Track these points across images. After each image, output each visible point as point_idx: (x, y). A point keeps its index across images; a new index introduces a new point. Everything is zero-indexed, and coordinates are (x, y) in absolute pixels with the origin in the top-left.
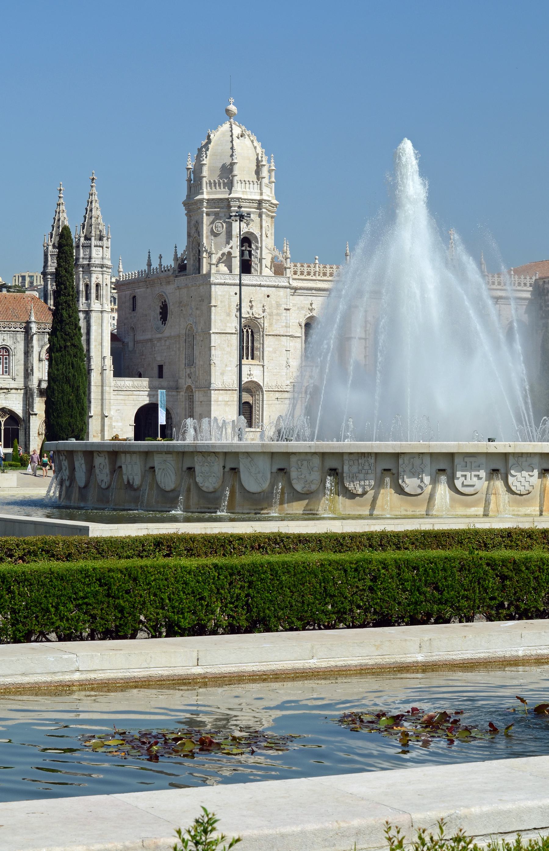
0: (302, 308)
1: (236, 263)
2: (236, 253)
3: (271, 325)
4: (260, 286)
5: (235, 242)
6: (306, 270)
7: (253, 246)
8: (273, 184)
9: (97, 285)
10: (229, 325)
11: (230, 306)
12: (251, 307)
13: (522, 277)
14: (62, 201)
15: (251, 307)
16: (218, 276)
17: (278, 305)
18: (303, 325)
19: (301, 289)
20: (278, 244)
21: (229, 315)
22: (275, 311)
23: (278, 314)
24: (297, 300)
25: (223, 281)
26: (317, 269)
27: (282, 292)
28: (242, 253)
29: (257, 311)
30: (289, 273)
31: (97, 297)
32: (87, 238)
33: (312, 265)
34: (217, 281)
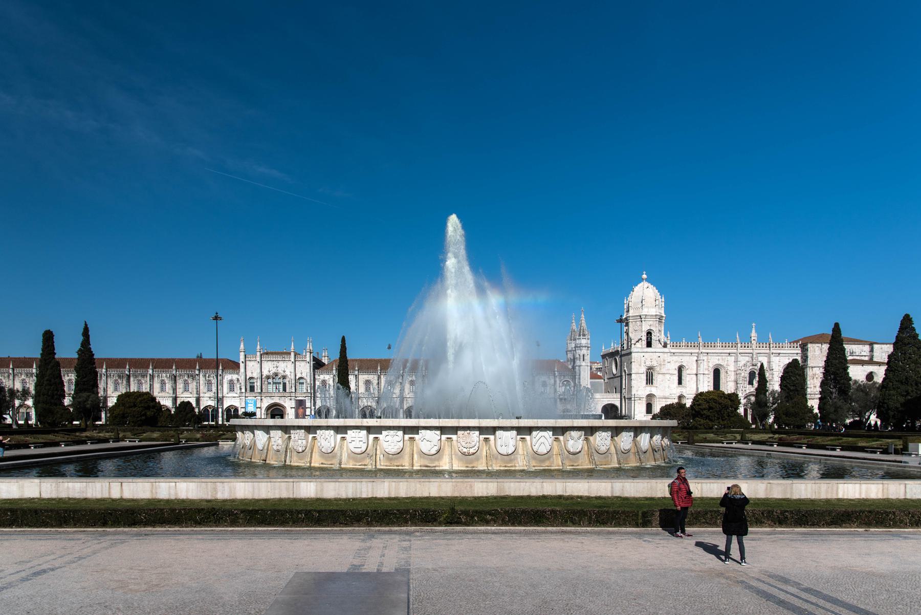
0: (676, 362)
1: (644, 343)
2: (644, 338)
3: (660, 369)
4: (655, 352)
5: (644, 334)
6: (689, 345)
7: (652, 335)
8: (663, 308)
9: (584, 355)
10: (640, 370)
11: (641, 361)
12: (651, 362)
13: (795, 344)
14: (573, 321)
15: (651, 362)
16: (635, 349)
17: (664, 361)
18: (677, 369)
19: (676, 353)
20: (665, 334)
21: (640, 365)
22: (662, 363)
23: (664, 365)
24: (675, 358)
25: (637, 351)
26: (684, 344)
27: (666, 355)
28: (647, 338)
29: (655, 364)
30: (668, 346)
31: (584, 360)
32: (580, 335)
33: (716, 343)
34: (634, 351)
